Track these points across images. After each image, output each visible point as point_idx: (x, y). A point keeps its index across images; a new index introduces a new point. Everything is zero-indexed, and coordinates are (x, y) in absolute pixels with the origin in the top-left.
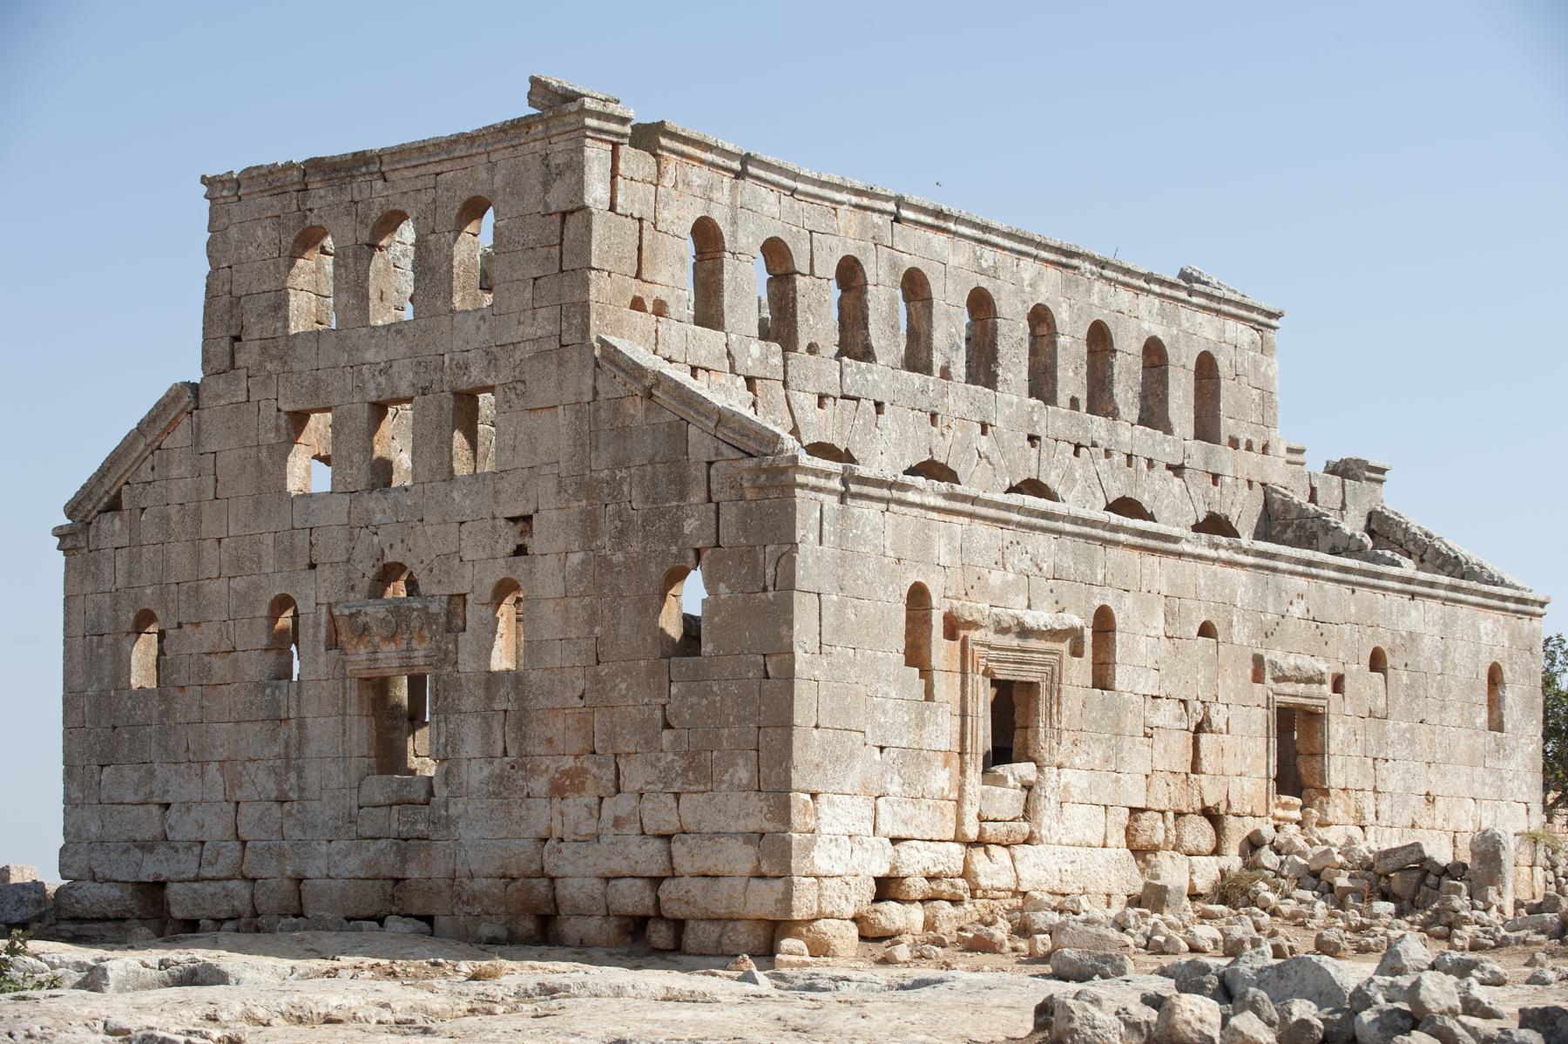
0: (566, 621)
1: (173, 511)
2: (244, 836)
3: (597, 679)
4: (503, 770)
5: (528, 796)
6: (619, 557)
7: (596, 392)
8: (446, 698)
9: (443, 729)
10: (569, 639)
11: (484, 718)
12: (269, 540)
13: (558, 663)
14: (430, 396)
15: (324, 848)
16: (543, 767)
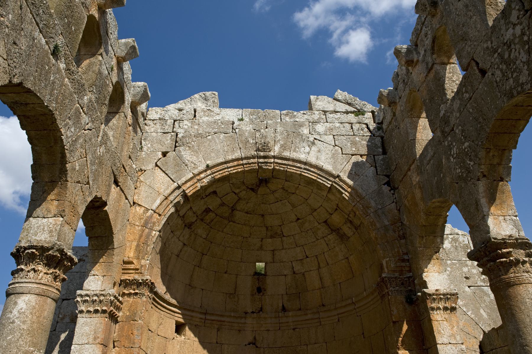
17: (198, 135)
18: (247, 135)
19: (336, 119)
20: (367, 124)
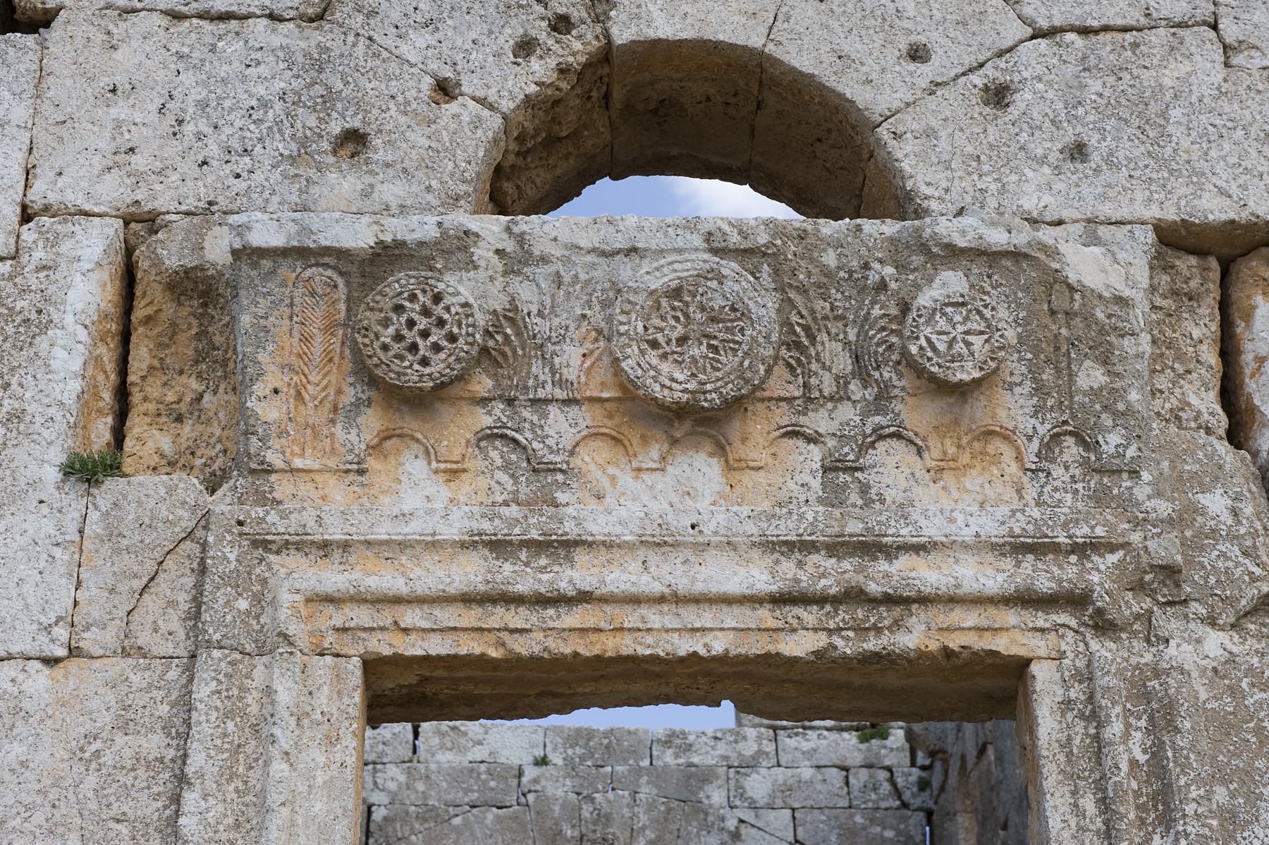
17: (429, 815)
18: (556, 815)
19: (804, 753)
20: (889, 769)
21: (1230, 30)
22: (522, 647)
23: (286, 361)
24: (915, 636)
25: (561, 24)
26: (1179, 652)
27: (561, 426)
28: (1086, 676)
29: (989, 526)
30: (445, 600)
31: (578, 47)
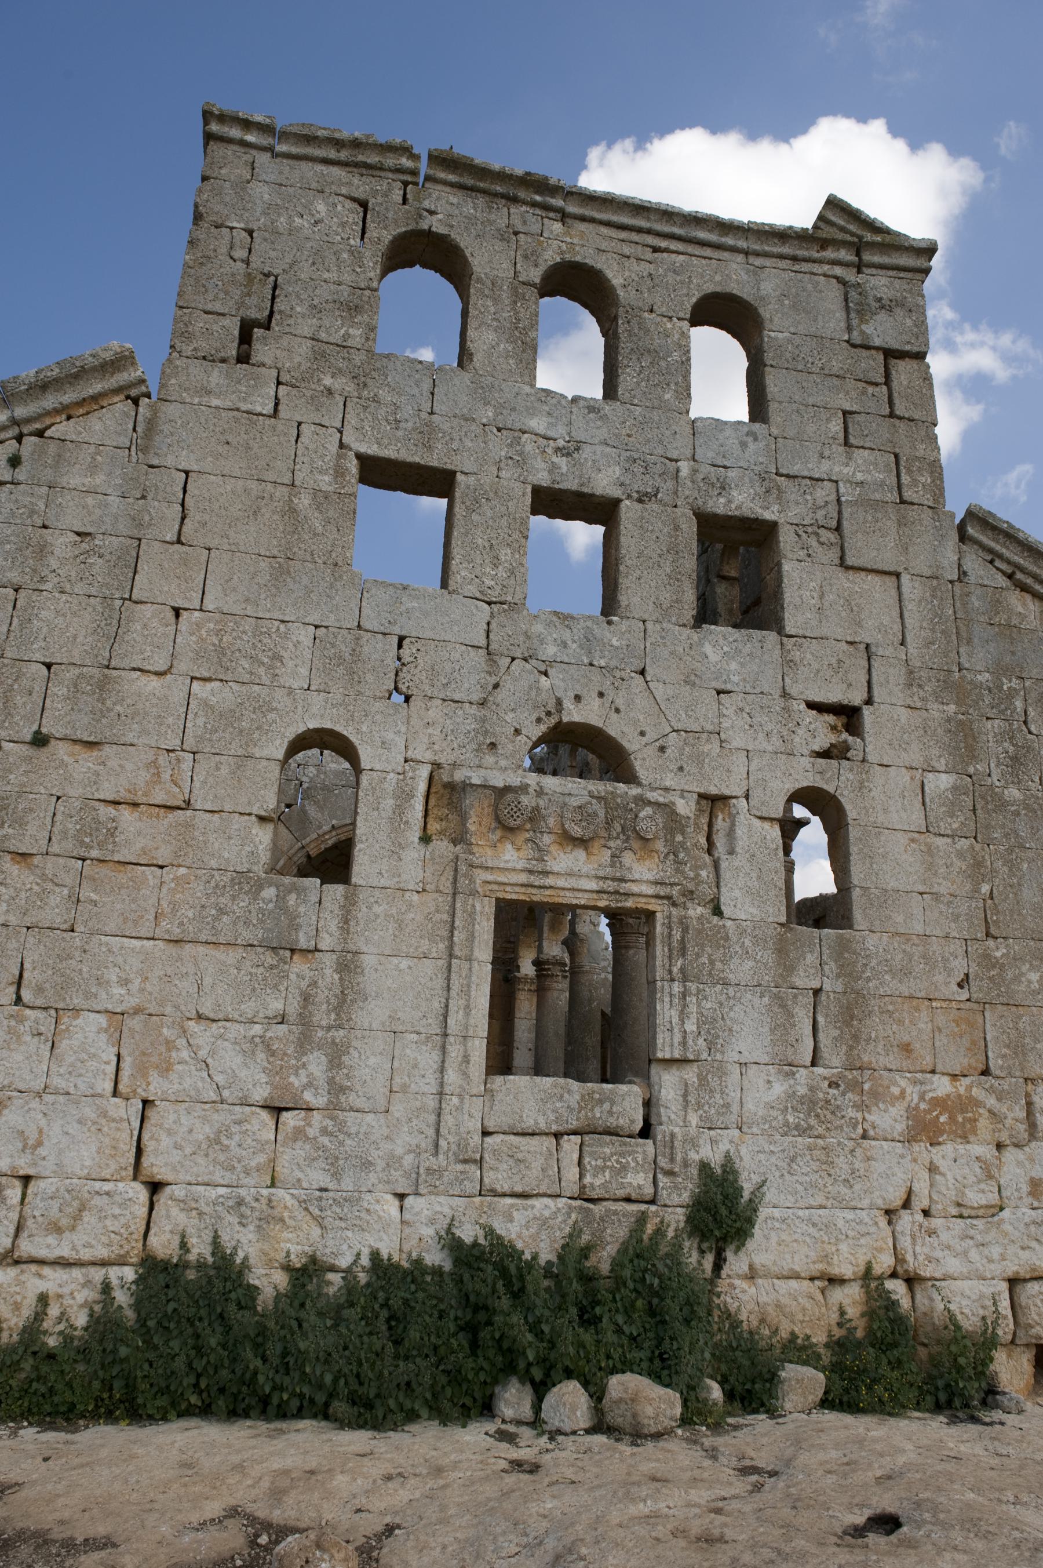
0: (930, 867)
1: (62, 544)
2: (156, 1165)
3: (987, 960)
4: (812, 1089)
5: (865, 1136)
6: (1013, 793)
7: (963, 574)
8: (698, 955)
9: (693, 1008)
10: (936, 896)
11: (777, 997)
12: (304, 635)
13: (919, 928)
14: (653, 506)
15: (392, 1206)
16: (895, 1091)
17: (325, 788)
21: (723, 736)
22: (535, 898)
23: (477, 817)
24: (629, 904)
25: (549, 714)
26: (691, 912)
27: (547, 839)
28: (669, 917)
29: (650, 876)
30: (516, 885)
31: (553, 721)
